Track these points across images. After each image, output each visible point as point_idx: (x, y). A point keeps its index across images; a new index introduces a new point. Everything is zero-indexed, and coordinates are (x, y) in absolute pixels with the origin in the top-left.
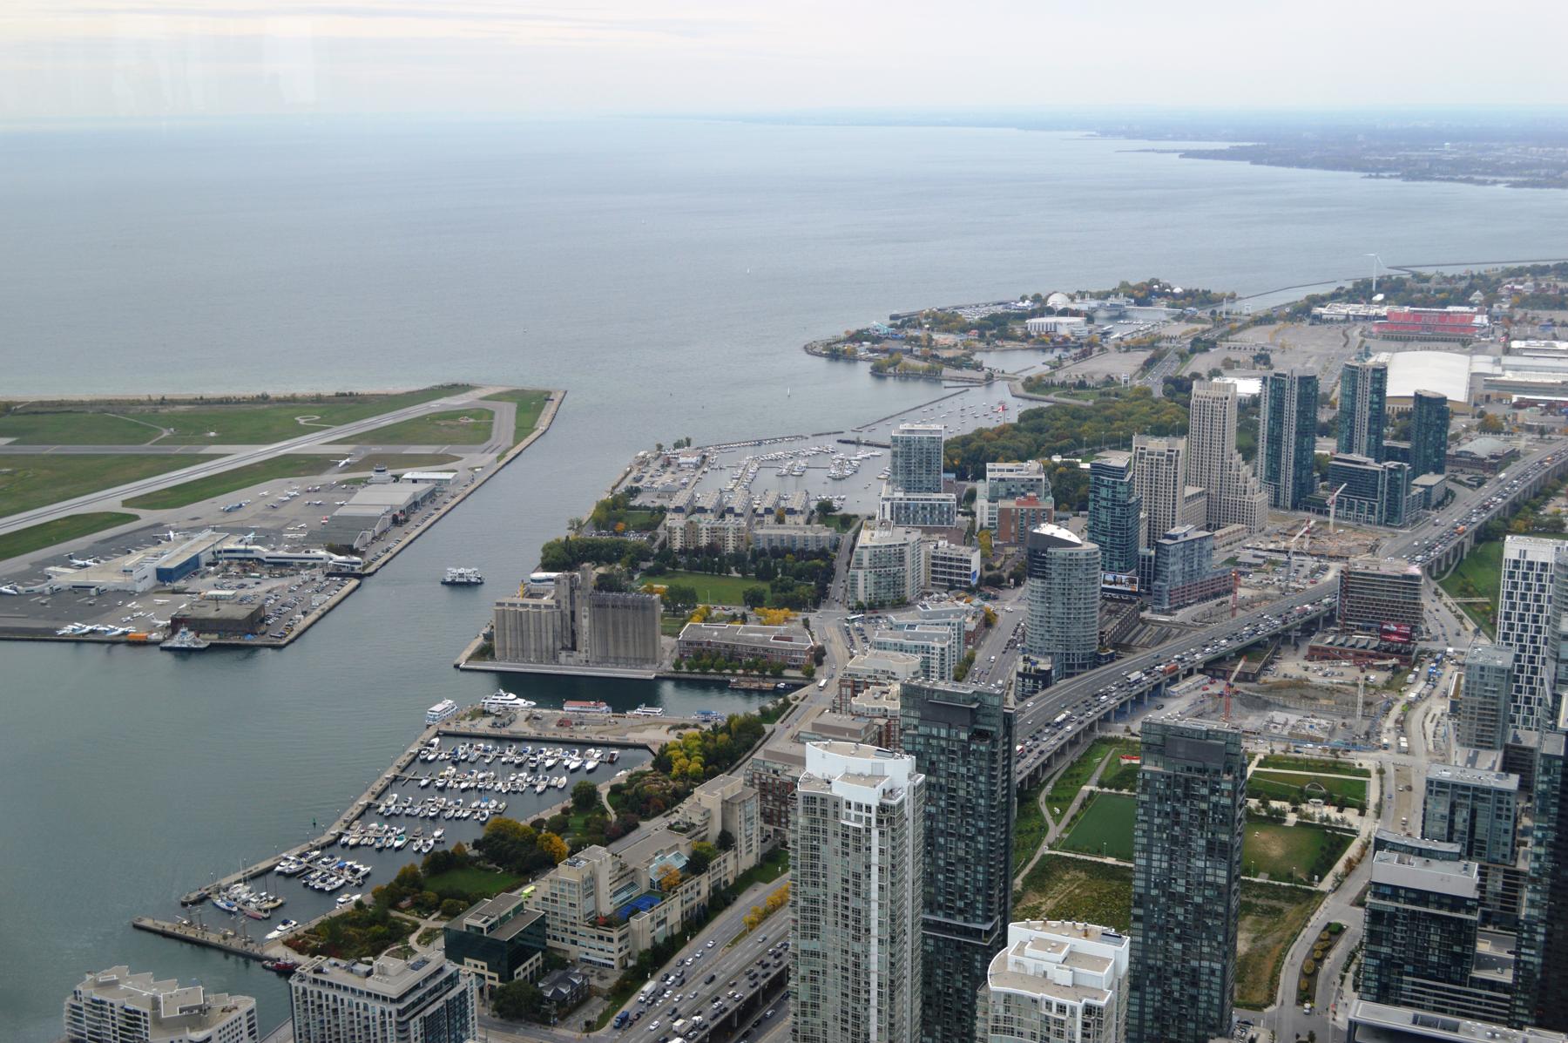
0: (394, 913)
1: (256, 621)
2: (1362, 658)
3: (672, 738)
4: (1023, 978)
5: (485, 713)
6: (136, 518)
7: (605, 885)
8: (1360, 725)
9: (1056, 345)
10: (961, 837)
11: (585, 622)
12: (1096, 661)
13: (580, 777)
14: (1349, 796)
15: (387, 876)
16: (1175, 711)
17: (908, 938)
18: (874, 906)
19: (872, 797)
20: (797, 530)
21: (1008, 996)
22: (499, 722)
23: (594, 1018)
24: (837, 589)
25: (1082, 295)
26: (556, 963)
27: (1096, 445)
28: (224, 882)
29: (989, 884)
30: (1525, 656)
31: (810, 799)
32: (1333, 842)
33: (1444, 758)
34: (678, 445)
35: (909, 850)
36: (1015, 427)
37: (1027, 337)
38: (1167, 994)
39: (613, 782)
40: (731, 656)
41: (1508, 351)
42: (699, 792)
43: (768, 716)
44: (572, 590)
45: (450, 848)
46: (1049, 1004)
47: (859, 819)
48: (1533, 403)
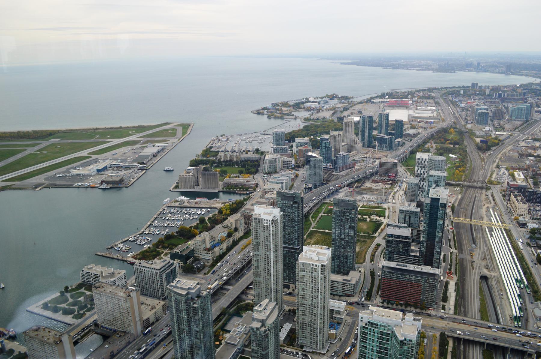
0: (158, 249)
1: (121, 181)
2: (384, 182)
3: (222, 206)
4: (307, 259)
5: (177, 201)
7: (208, 241)
8: (384, 198)
9: (311, 110)
10: (291, 227)
11: (201, 179)
12: (322, 184)
13: (201, 216)
14: (381, 214)
15: (156, 241)
16: (341, 196)
17: (280, 251)
18: (272, 243)
19: (270, 218)
20: (251, 155)
21: (303, 263)
23: (206, 272)
24: (261, 168)
25: (317, 98)
26: (197, 259)
27: (322, 133)
28: (117, 243)
29: (298, 237)
30: (421, 180)
31: (256, 219)
32: (378, 225)
33: (403, 205)
34: (221, 136)
35: (279, 230)
36: (302, 130)
37: (304, 108)
38: (340, 261)
40: (236, 186)
41: (417, 109)
42: (229, 218)
43: (245, 200)
45: (170, 233)
46: (313, 265)
47: (267, 223)
48: (423, 121)
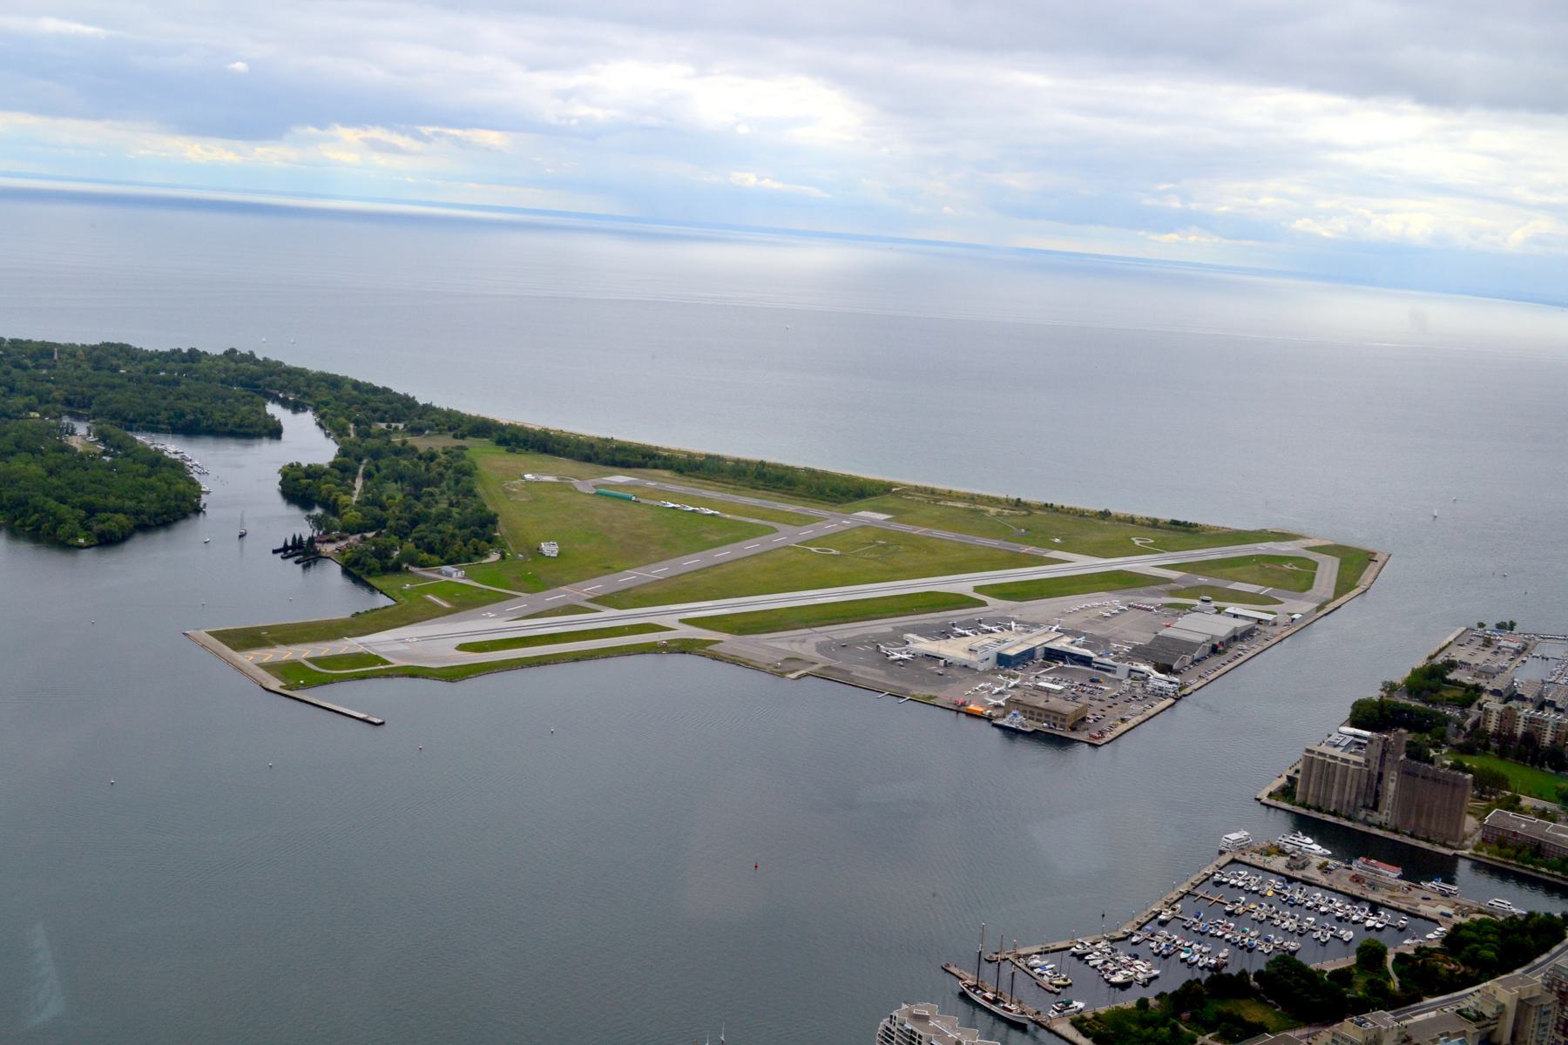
1: (1080, 722)
5: (1282, 852)
6: (984, 604)
11: (1392, 786)
22: (1294, 863)
28: (1022, 952)
39: (1400, 949)
40: (1537, 850)
44: (1384, 753)
45: (1233, 970)
